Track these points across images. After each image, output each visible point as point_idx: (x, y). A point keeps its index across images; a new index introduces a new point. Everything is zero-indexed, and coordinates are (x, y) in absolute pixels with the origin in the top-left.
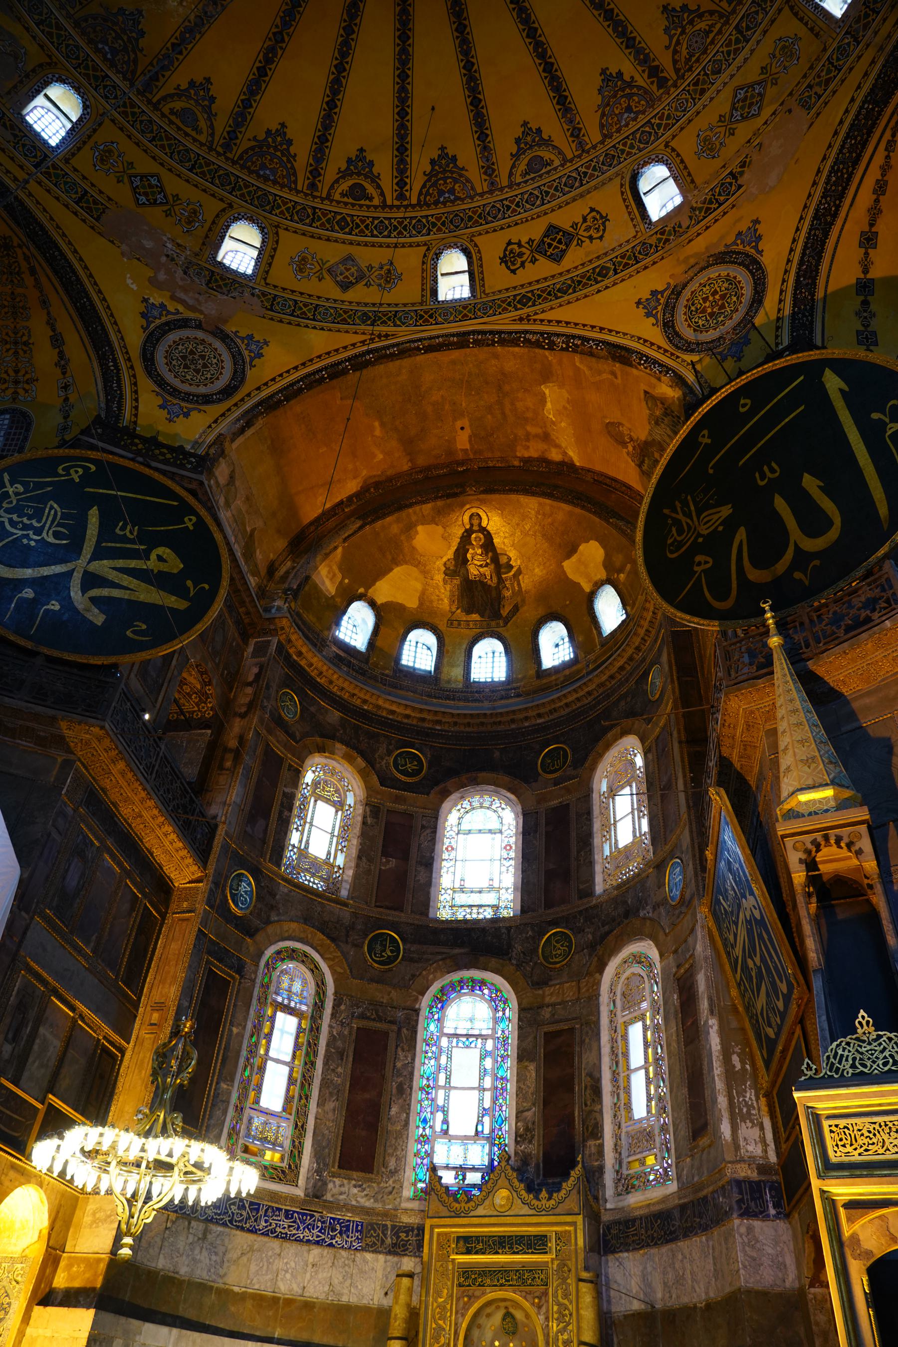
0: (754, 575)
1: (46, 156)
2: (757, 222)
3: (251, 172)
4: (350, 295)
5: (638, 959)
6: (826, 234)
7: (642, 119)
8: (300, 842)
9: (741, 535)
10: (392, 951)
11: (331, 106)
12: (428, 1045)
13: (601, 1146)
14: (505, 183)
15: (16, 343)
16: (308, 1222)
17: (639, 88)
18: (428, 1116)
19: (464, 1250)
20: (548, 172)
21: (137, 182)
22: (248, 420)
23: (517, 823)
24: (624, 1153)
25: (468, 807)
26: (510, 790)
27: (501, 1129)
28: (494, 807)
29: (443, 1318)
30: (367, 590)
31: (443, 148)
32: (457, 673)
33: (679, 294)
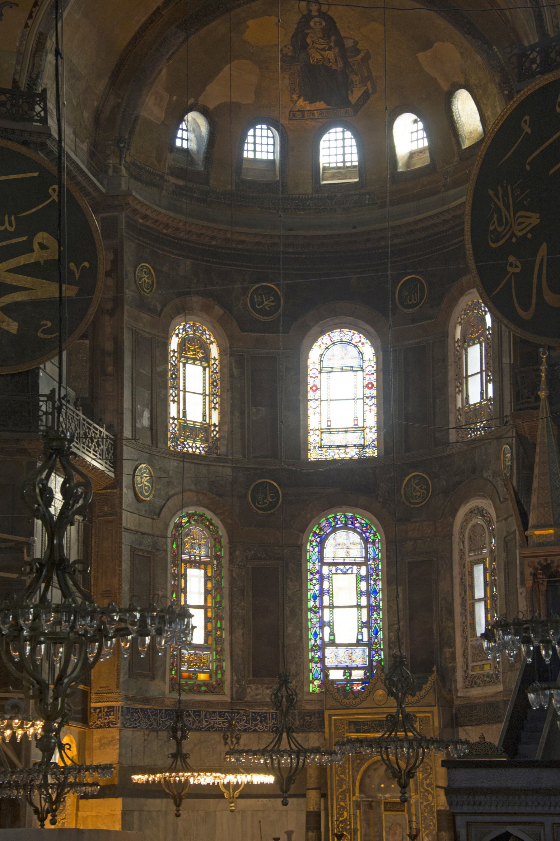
5: (481, 512)
8: (178, 412)
10: (272, 497)
12: (312, 574)
13: (454, 653)
16: (236, 718)
18: (318, 631)
19: (354, 730)
23: (377, 358)
24: (470, 659)
25: (329, 343)
26: (368, 322)
27: (376, 638)
28: (354, 342)
29: (343, 773)
30: (196, 100)
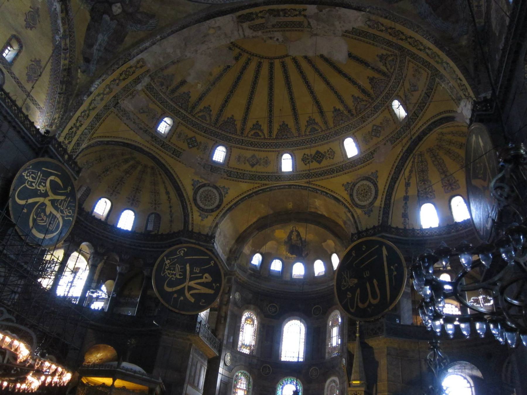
0: (360, 305)
1: (164, 142)
2: (377, 171)
3: (223, 130)
4: (254, 169)
5: (334, 381)
6: (395, 183)
7: (346, 124)
9: (359, 290)
11: (248, 109)
14: (303, 134)
15: (155, 193)
17: (345, 115)
20: (317, 133)
21: (189, 141)
22: (224, 215)
31: (283, 122)
32: (288, 275)
33: (355, 186)
